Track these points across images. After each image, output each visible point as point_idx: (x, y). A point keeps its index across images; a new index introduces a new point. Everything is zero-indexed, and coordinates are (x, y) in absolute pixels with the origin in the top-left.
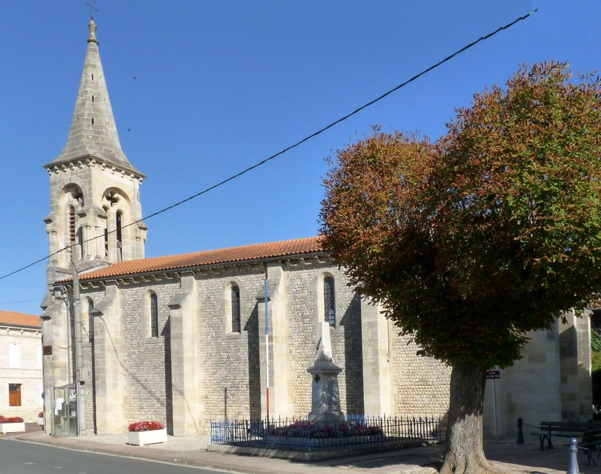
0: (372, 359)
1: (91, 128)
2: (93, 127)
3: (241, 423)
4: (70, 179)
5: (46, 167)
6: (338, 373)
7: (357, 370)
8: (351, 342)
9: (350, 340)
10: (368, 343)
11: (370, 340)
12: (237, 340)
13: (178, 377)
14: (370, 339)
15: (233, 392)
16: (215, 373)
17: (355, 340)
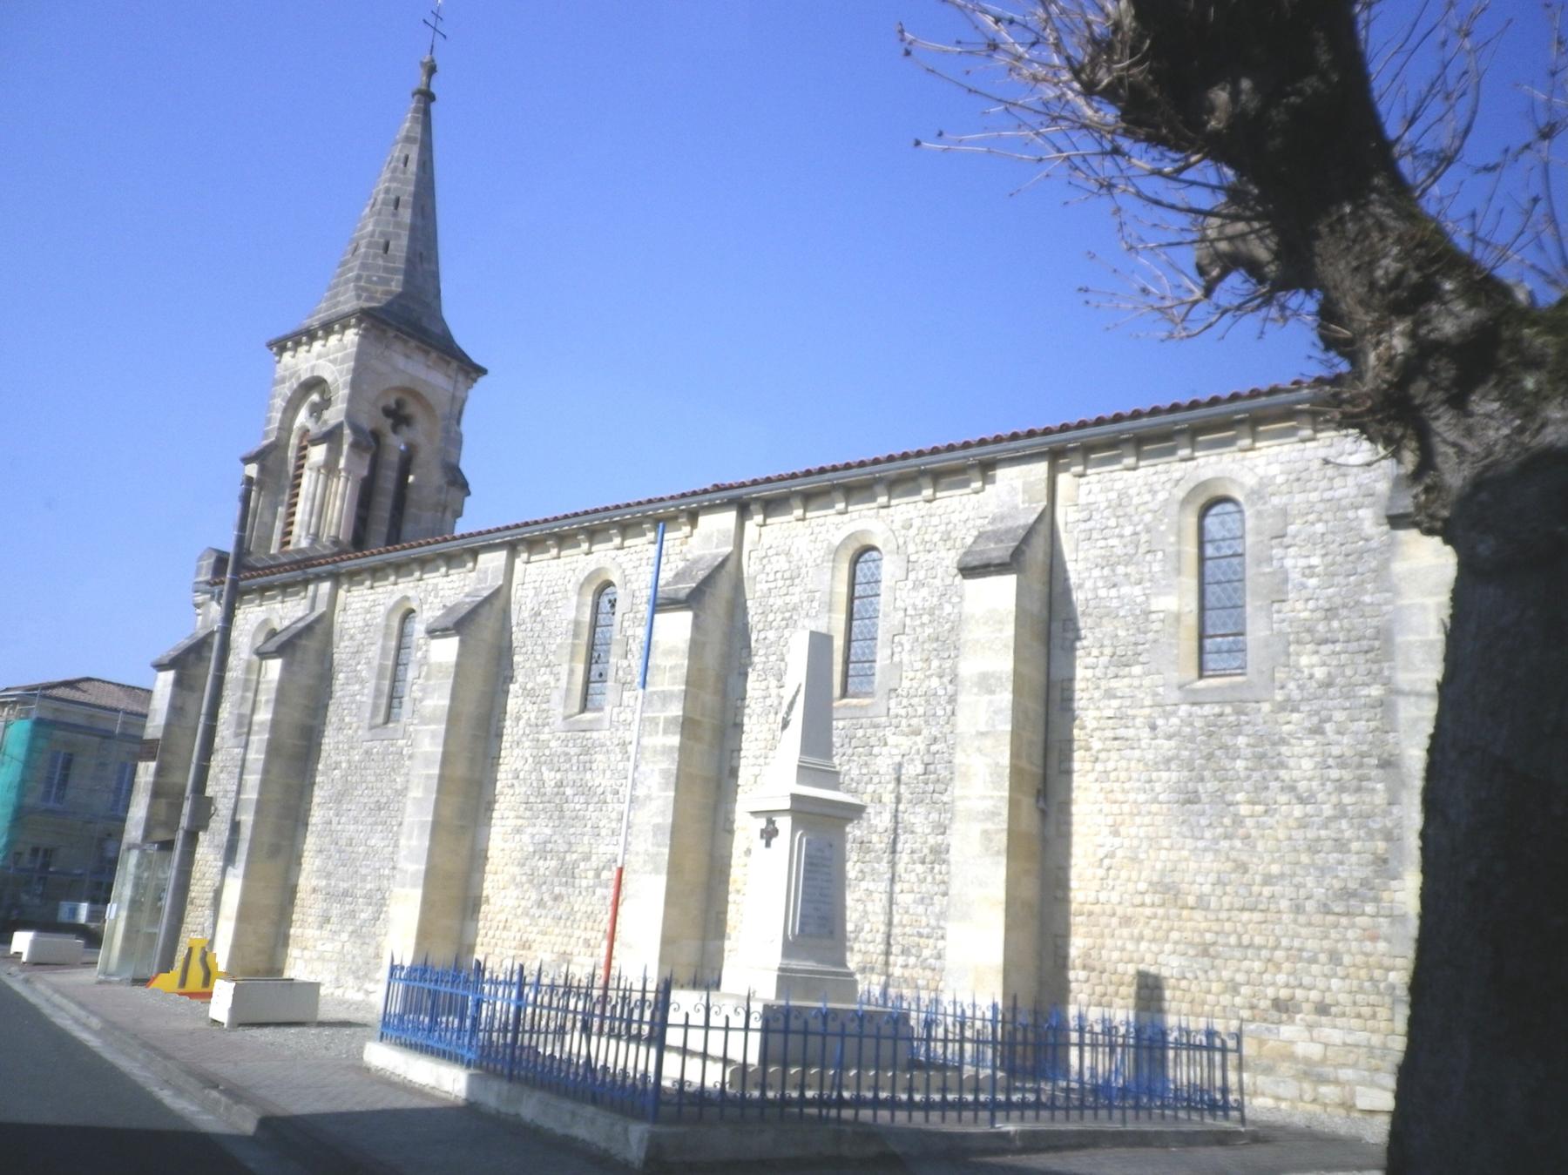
0: (984, 798)
1: (380, 262)
2: (385, 260)
3: (501, 977)
4: (313, 368)
5: (270, 345)
6: (851, 820)
7: (932, 840)
8: (922, 747)
9: (919, 739)
10: (976, 743)
11: (982, 734)
12: (588, 735)
13: (416, 832)
14: (983, 729)
15: (557, 890)
16: (518, 830)
17: (935, 740)
